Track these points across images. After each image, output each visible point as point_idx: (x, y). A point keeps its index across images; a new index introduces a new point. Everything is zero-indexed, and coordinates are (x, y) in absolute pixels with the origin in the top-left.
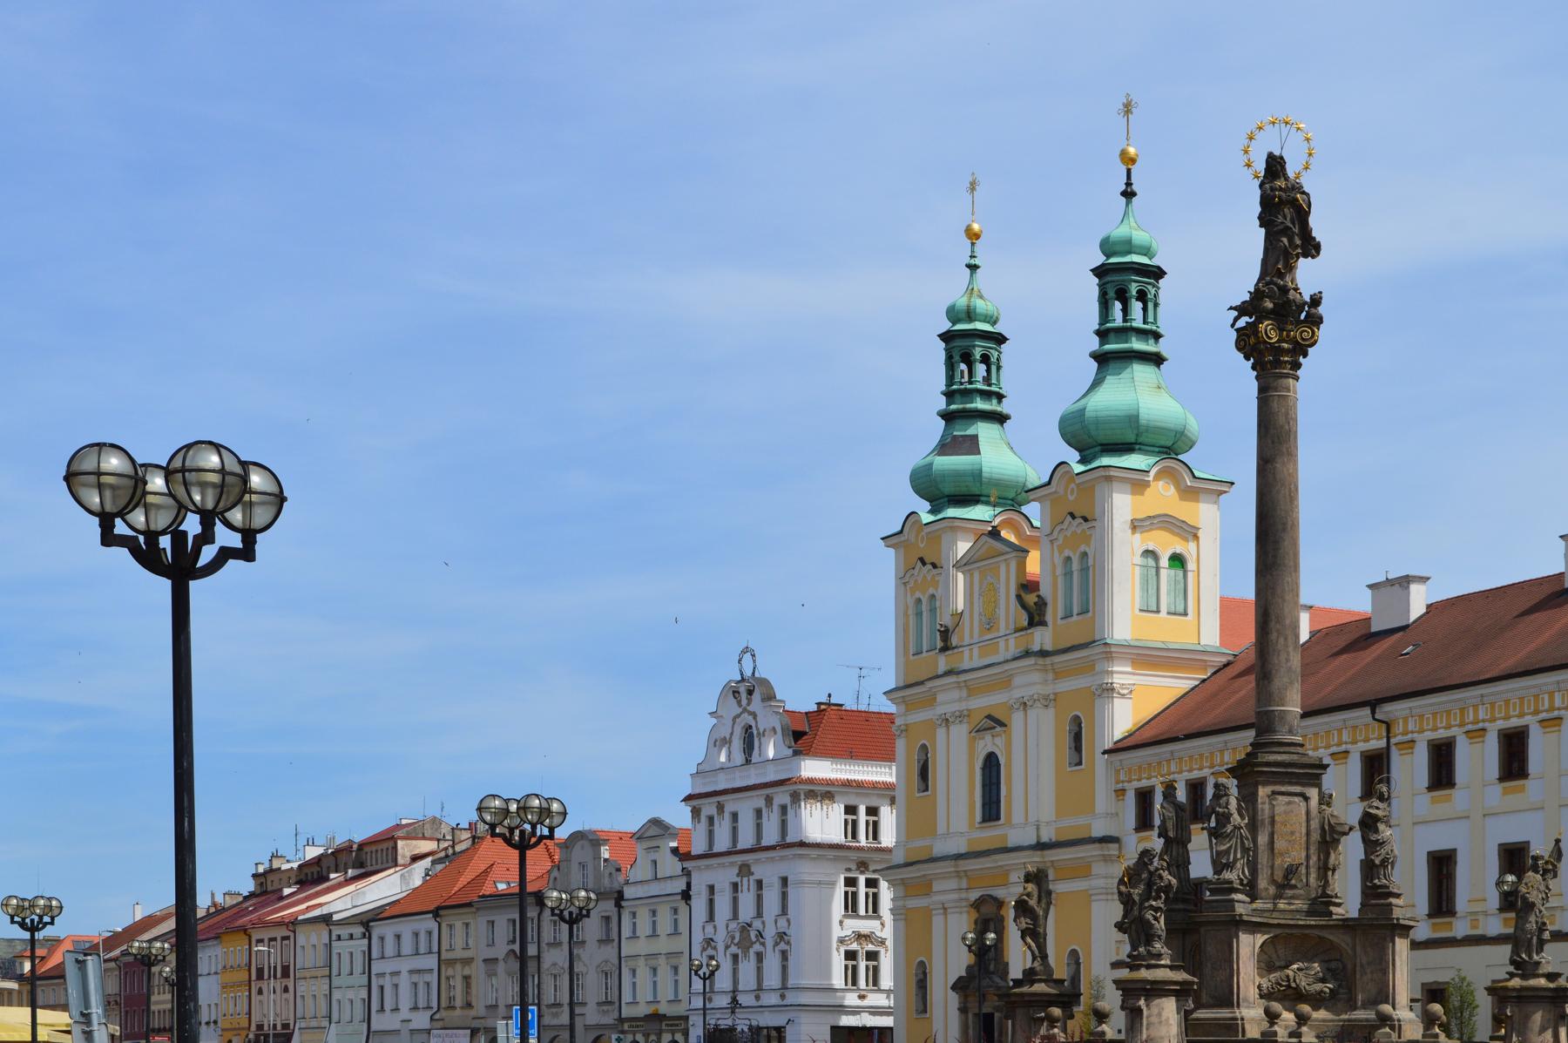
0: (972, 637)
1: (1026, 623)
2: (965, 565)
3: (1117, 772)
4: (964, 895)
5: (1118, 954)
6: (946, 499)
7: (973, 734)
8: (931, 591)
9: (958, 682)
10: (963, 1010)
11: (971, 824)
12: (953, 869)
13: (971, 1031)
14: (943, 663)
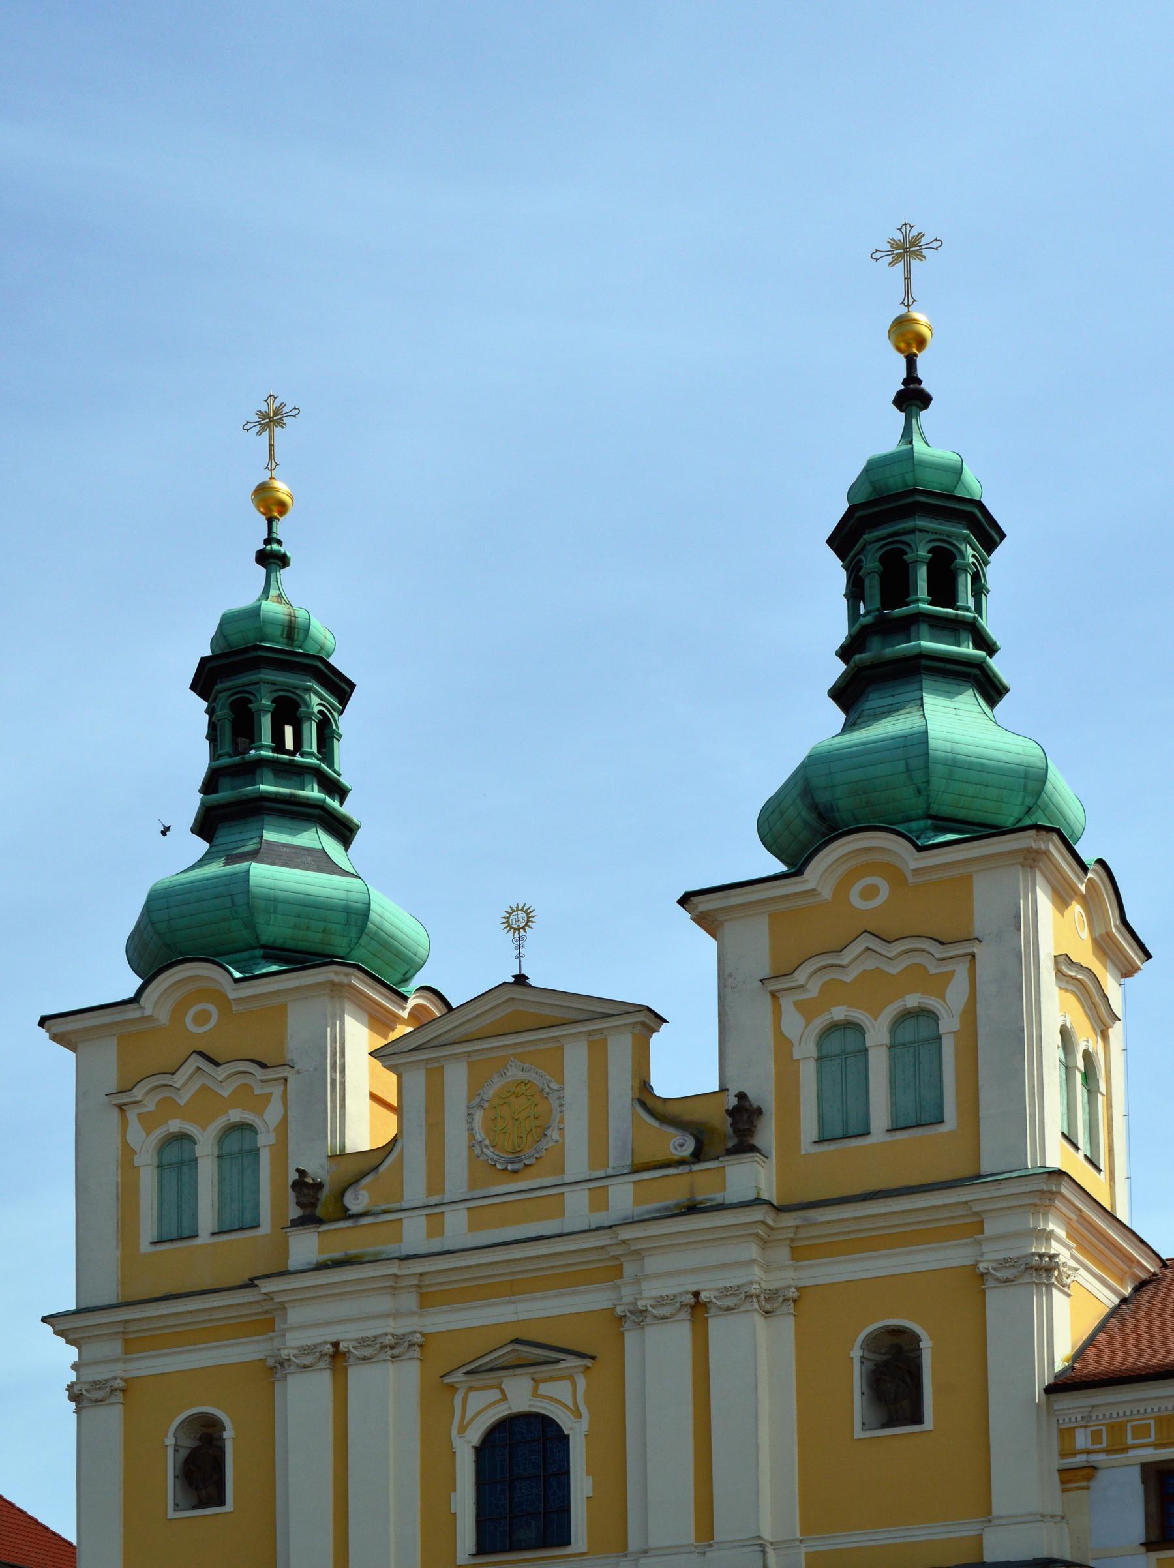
3: (1066, 1434)
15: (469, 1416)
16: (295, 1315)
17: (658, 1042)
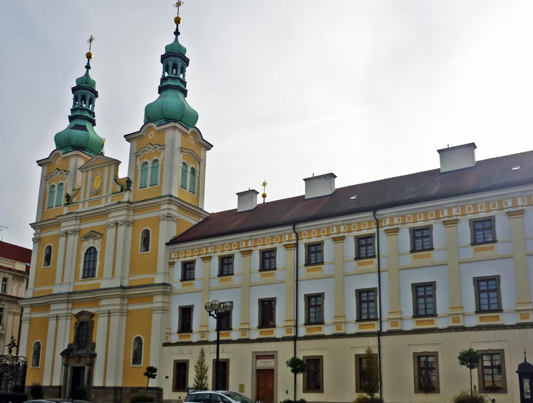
0: (85, 197)
1: (119, 190)
2: (85, 168)
4: (70, 311)
5: (166, 339)
6: (71, 147)
7: (83, 239)
8: (61, 182)
9: (76, 217)
10: (66, 365)
11: (76, 279)
12: (66, 299)
13: (69, 375)
14: (66, 210)
15: (84, 247)
16: (63, 224)
17: (120, 166)
